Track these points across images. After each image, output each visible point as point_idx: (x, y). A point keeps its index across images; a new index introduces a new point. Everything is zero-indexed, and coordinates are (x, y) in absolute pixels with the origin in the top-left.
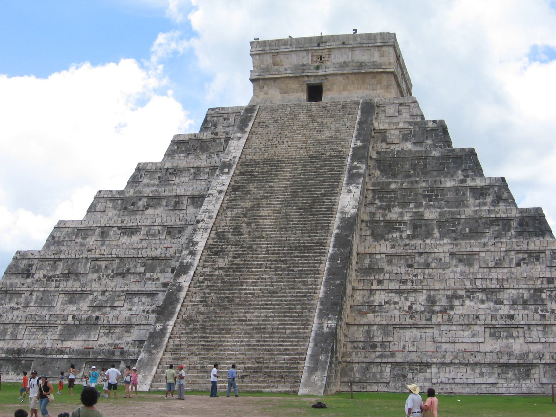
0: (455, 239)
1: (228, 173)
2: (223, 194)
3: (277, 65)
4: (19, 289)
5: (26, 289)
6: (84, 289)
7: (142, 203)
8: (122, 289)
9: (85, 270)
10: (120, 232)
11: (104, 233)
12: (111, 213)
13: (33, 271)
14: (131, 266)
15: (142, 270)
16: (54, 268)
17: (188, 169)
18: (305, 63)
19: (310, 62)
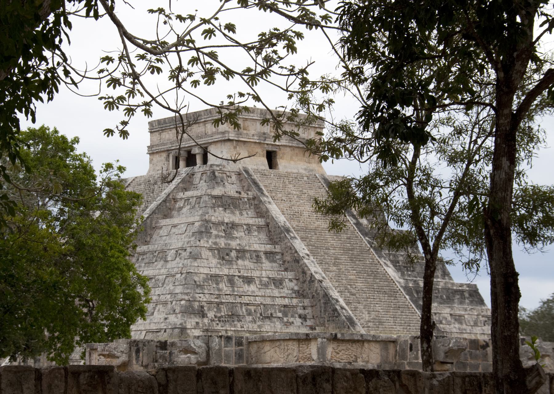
0: (441, 303)
1: (295, 238)
2: (312, 258)
3: (246, 130)
4: (216, 328)
5: (221, 328)
6: (262, 330)
7: (233, 254)
8: (286, 331)
9: (243, 313)
10: (241, 280)
11: (231, 280)
12: (214, 261)
13: (206, 312)
14: (273, 311)
15: (280, 315)
16: (219, 310)
17: (241, 225)
18: (265, 132)
19: (269, 131)
